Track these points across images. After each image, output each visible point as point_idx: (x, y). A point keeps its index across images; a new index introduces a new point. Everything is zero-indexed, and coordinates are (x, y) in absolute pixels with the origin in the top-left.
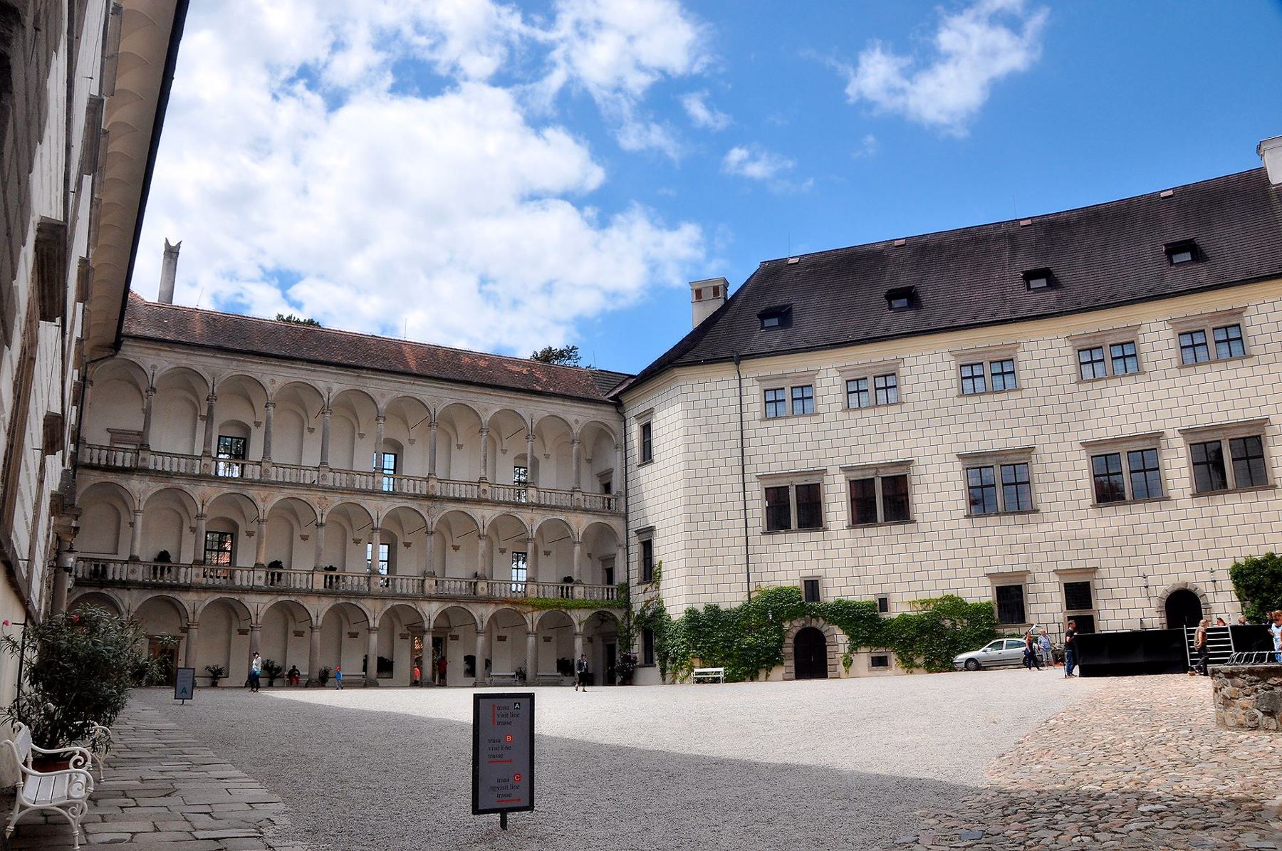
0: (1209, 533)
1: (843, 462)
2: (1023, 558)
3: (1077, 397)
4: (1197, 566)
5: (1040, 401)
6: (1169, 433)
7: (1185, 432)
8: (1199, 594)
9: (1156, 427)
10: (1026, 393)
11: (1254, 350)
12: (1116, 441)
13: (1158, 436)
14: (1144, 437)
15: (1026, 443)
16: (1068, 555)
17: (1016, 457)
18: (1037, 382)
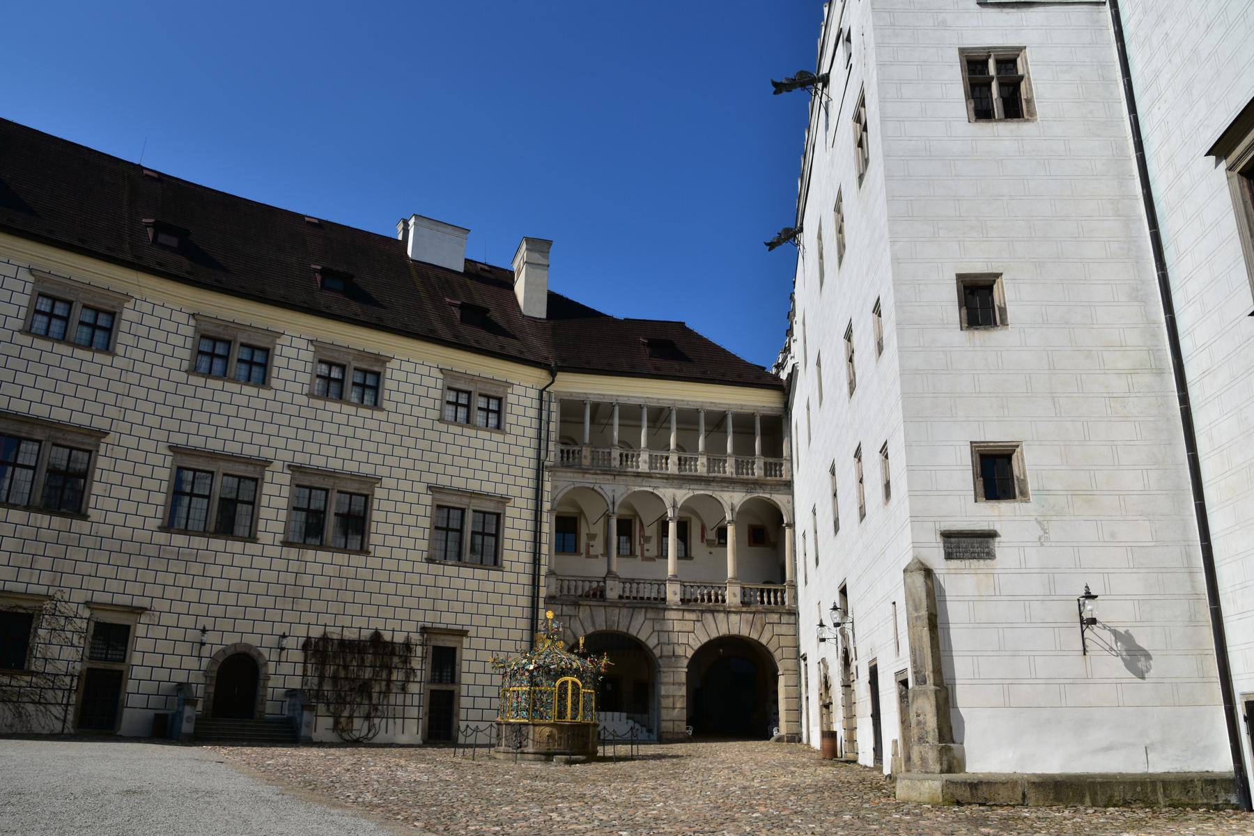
0: (290, 591)
2: (46, 578)
3: (183, 390)
4: (266, 628)
5: (133, 379)
6: (277, 465)
7: (295, 469)
8: (261, 661)
9: (267, 453)
10: (118, 362)
11: (386, 405)
12: (214, 456)
13: (266, 463)
14: (248, 461)
15: (99, 423)
16: (114, 586)
17: (79, 438)
18: (138, 354)
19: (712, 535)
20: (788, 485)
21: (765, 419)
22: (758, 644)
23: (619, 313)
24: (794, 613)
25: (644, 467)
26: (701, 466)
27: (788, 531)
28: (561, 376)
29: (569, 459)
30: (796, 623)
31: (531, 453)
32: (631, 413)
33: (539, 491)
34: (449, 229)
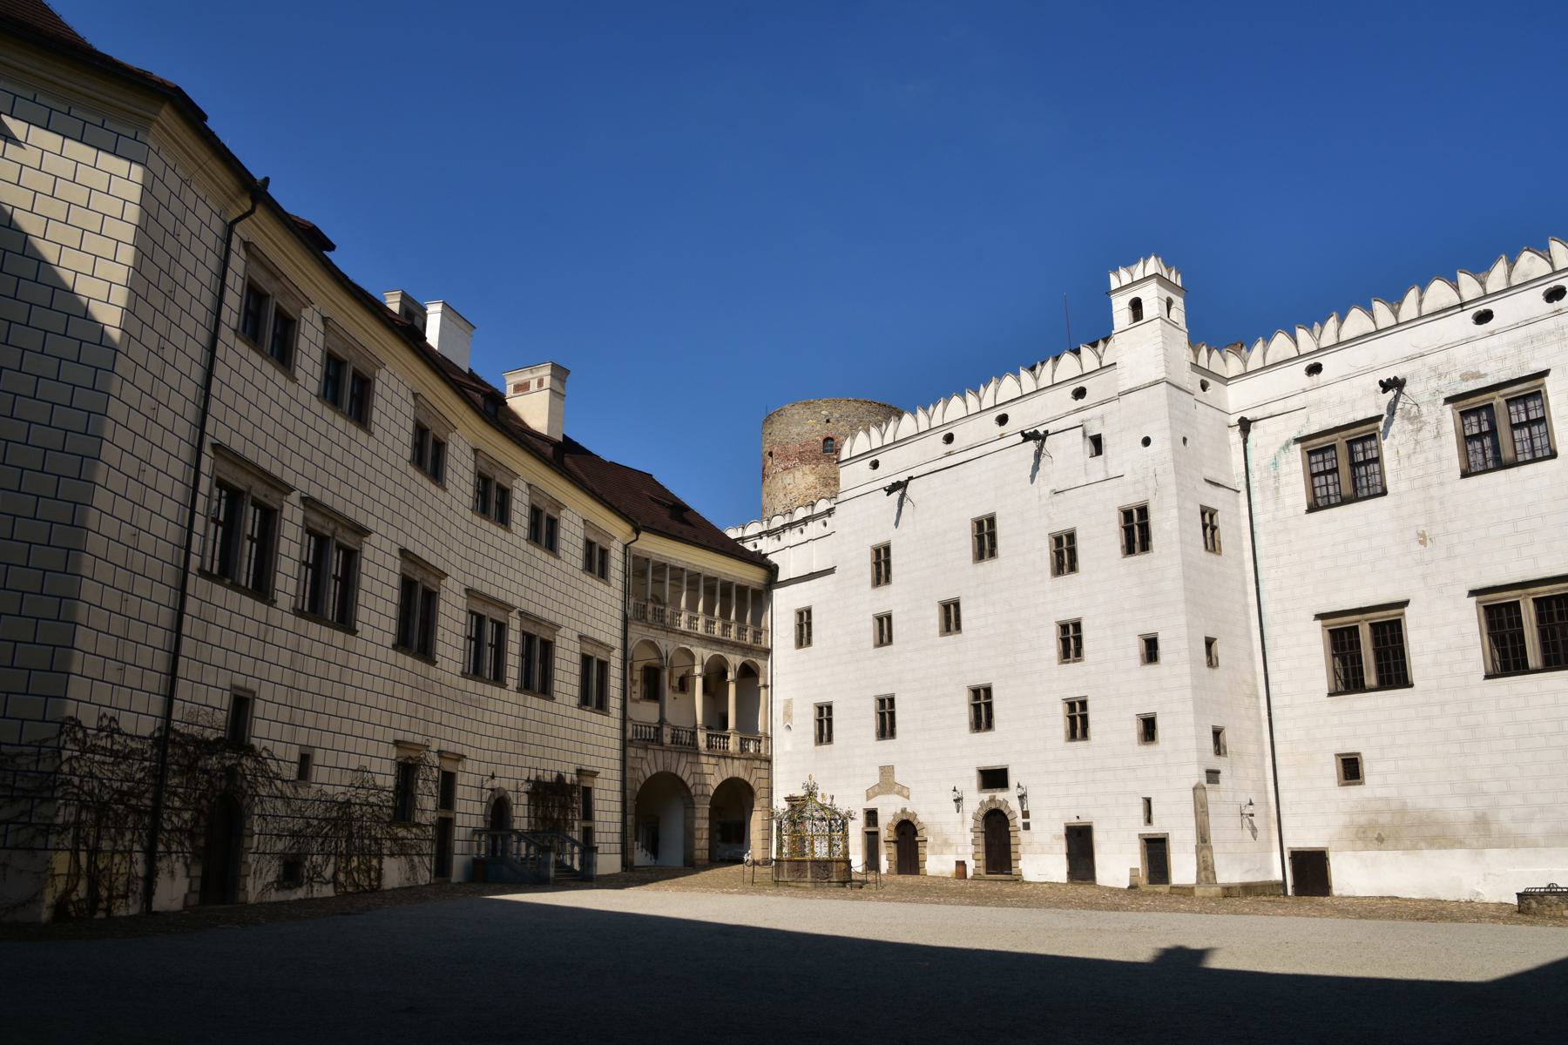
1: (315, 493)
19: (676, 683)
20: (768, 652)
21: (754, 591)
22: (747, 784)
23: (607, 456)
24: (769, 761)
25: (684, 626)
26: (717, 632)
27: (763, 691)
28: (643, 535)
29: (641, 616)
30: (770, 770)
31: (620, 605)
32: (677, 573)
33: (625, 639)
34: (462, 323)
